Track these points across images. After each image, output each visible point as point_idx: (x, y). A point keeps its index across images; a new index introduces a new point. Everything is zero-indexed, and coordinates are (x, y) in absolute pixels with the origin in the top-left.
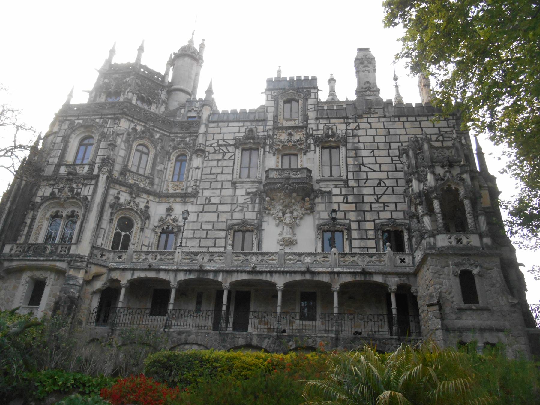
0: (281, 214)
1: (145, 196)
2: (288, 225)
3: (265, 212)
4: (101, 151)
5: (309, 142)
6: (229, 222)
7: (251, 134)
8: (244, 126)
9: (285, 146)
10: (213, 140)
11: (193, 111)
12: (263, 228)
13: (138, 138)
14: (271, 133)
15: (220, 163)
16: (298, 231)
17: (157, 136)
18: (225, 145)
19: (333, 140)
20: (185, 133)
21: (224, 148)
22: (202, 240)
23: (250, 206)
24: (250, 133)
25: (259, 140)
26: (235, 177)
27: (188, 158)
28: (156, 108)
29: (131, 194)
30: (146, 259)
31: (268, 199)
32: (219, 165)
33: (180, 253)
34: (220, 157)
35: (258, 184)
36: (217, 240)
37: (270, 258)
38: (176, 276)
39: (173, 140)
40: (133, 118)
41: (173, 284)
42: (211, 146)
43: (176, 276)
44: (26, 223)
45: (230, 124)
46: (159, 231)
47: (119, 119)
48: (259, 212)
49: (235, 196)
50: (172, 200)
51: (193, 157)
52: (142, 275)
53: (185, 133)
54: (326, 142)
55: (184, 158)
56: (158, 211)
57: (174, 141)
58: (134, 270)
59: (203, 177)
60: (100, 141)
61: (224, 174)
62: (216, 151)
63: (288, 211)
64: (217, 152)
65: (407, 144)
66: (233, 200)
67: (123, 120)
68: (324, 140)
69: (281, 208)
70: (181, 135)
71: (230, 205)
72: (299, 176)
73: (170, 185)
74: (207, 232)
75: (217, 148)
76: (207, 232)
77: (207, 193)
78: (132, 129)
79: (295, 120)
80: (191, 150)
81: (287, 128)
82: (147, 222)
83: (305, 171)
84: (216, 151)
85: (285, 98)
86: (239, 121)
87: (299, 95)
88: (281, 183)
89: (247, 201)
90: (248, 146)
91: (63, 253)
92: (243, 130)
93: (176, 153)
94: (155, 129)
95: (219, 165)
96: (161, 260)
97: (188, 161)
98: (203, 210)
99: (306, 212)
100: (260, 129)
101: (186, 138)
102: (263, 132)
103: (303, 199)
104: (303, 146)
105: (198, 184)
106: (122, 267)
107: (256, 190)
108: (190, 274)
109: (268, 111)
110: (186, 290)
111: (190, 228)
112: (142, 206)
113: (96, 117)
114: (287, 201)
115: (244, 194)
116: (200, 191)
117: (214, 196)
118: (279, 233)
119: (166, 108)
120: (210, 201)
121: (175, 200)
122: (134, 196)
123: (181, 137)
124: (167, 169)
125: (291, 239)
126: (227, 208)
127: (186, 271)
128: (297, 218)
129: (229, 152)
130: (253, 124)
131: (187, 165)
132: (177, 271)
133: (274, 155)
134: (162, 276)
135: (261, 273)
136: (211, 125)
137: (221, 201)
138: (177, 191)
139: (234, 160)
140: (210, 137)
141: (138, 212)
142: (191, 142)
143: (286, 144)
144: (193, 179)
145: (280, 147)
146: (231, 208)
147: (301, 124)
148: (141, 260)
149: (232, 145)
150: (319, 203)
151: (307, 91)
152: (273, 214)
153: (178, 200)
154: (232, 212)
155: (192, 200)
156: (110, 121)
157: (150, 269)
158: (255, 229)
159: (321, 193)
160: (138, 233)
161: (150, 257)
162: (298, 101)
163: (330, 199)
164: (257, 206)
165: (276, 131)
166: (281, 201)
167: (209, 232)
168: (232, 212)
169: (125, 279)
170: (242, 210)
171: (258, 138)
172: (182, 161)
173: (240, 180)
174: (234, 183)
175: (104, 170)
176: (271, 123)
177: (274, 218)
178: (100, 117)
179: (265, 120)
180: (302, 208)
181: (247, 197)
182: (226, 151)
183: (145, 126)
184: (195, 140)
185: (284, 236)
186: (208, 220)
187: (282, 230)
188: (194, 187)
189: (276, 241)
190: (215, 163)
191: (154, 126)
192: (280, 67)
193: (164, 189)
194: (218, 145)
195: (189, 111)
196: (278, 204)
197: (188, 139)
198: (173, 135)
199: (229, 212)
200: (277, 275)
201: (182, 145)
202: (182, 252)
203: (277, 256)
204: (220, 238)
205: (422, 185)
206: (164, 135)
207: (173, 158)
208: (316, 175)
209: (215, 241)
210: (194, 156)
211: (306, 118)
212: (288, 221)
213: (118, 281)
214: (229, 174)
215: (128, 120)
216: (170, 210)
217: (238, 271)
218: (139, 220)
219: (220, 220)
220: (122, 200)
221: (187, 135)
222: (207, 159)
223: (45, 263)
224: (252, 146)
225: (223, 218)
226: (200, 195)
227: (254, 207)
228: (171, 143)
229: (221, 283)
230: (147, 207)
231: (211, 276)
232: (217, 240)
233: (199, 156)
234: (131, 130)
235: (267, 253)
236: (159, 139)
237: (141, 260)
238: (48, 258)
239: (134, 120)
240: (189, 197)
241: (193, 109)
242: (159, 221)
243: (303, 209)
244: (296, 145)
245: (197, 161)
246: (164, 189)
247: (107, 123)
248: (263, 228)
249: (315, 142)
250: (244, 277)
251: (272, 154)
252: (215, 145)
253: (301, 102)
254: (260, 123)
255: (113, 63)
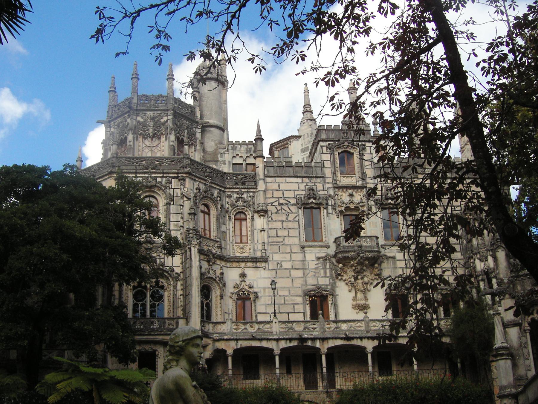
0: (353, 279)
1: (218, 262)
2: (362, 291)
3: (337, 278)
4: (173, 217)
5: (370, 204)
6: (304, 288)
7: (311, 193)
8: (302, 183)
9: (347, 208)
10: (273, 197)
11: (238, 157)
12: (337, 293)
13: (202, 198)
14: (331, 192)
15: (285, 224)
16: (370, 295)
17: (216, 194)
18: (287, 204)
19: (393, 202)
20: (241, 188)
21: (285, 208)
22: (281, 306)
23: (322, 272)
24: (311, 192)
25: (321, 201)
26: (302, 240)
27: (249, 217)
28: (195, 151)
29: (208, 262)
30: (246, 329)
31: (341, 265)
32: (284, 227)
33: (277, 322)
34: (284, 218)
35: (326, 249)
36: (296, 306)
37: (358, 325)
38: (278, 344)
39: (229, 197)
40: (195, 176)
41: (277, 351)
42: (272, 205)
43: (278, 344)
44: (115, 295)
45: (289, 180)
46: (235, 297)
47: (184, 180)
48: (331, 276)
49: (305, 260)
50: (243, 265)
51: (255, 217)
52: (245, 344)
53: (241, 188)
54: (386, 204)
55: (243, 216)
56: (232, 275)
57: (231, 197)
58: (237, 340)
59: (272, 240)
60: (168, 204)
61: (291, 237)
62: (278, 211)
63: (359, 277)
64: (280, 212)
65: (459, 208)
66: (304, 265)
67: (187, 180)
68: (384, 203)
69: (353, 274)
70: (237, 190)
71: (302, 270)
72: (369, 244)
73: (236, 248)
74: (284, 298)
75: (279, 208)
76: (284, 298)
77: (277, 257)
78: (196, 189)
79: (352, 177)
80: (252, 209)
81: (347, 188)
82: (224, 288)
83: (375, 238)
84: (278, 211)
85: (340, 151)
86: (297, 177)
87: (355, 148)
88: (354, 251)
89: (318, 266)
90: (310, 206)
91: (171, 327)
92: (302, 187)
93: (235, 211)
94: (213, 185)
95: (284, 227)
96: (259, 329)
97: (248, 221)
98: (277, 276)
99: (375, 277)
100: (320, 187)
101: (243, 194)
102: (323, 190)
103: (372, 265)
104: (365, 209)
105: (266, 248)
106: (225, 337)
107: (325, 254)
108: (290, 342)
109: (326, 166)
110: (288, 356)
111: (267, 294)
112: (218, 272)
113: (156, 175)
114: (359, 268)
115: (314, 259)
116: (271, 256)
117: (285, 261)
118: (352, 298)
119: (204, 150)
120: (281, 266)
121: (246, 265)
122: (211, 264)
123: (238, 194)
124: (229, 229)
125: (365, 304)
126: (300, 273)
127: (286, 339)
128: (367, 283)
129: (292, 213)
130: (312, 181)
131: (249, 225)
132: (278, 340)
133: (338, 217)
134: (264, 344)
135: (353, 338)
136: (269, 180)
137: (292, 267)
138: (244, 255)
139: (298, 221)
140: (269, 195)
141: (217, 280)
142: (250, 199)
143: (348, 205)
144: (260, 242)
145: (343, 209)
146: (304, 274)
147: (359, 184)
148: (240, 330)
149: (292, 205)
150: (385, 268)
151: (364, 145)
152: (345, 280)
153: (249, 264)
154: (305, 277)
155: (263, 264)
156: (173, 180)
157: (254, 339)
158: (330, 295)
159: (387, 259)
160: (219, 302)
161: (248, 326)
162: (353, 154)
163: (394, 263)
164: (328, 271)
165: (336, 190)
166: (354, 268)
167: (286, 298)
168: (305, 277)
169: (230, 348)
170: (315, 276)
171: (320, 198)
172: (241, 220)
173: (307, 244)
174: (303, 247)
175: (194, 243)
176: (329, 180)
177: (347, 284)
178: (162, 175)
179: (323, 177)
180: (372, 273)
181: (317, 262)
182: (289, 211)
183: (205, 184)
184: (253, 197)
185: (358, 302)
186: (283, 286)
187: (354, 295)
188: (263, 251)
189: (351, 306)
190: (279, 225)
191: (211, 183)
192: (306, 84)
193: (231, 253)
194: (280, 204)
195: (234, 157)
196: (350, 269)
197: (245, 196)
198: (228, 190)
199: (302, 278)
200: (366, 340)
201: (240, 203)
202: (279, 322)
203: (363, 323)
204: (298, 304)
205: (482, 264)
206: (220, 190)
207: (233, 217)
208: (381, 241)
209: (294, 307)
210: (256, 216)
211: (363, 177)
212: (360, 286)
213: (224, 351)
214: (296, 237)
215: (192, 179)
216: (243, 275)
217: (332, 338)
218: (218, 287)
219: (295, 285)
220: (203, 270)
221: (244, 190)
222: (270, 219)
223: (157, 337)
224: (313, 205)
225: (298, 283)
226: (270, 259)
227: (325, 273)
228: (227, 199)
229: (319, 349)
230: (222, 274)
231: (309, 343)
232: (296, 306)
233: (262, 217)
234: (195, 191)
235: (354, 321)
236: (218, 197)
237: (240, 330)
238: (160, 333)
239: (197, 179)
240: (261, 262)
241: (238, 155)
242: (234, 287)
243: (373, 275)
244: (358, 207)
245: (260, 222)
246: (231, 253)
247: (171, 183)
248: (337, 293)
249: (376, 204)
250: (339, 342)
251: (336, 217)
252: (276, 203)
253: (356, 155)
254: (319, 180)
255: (140, 93)
